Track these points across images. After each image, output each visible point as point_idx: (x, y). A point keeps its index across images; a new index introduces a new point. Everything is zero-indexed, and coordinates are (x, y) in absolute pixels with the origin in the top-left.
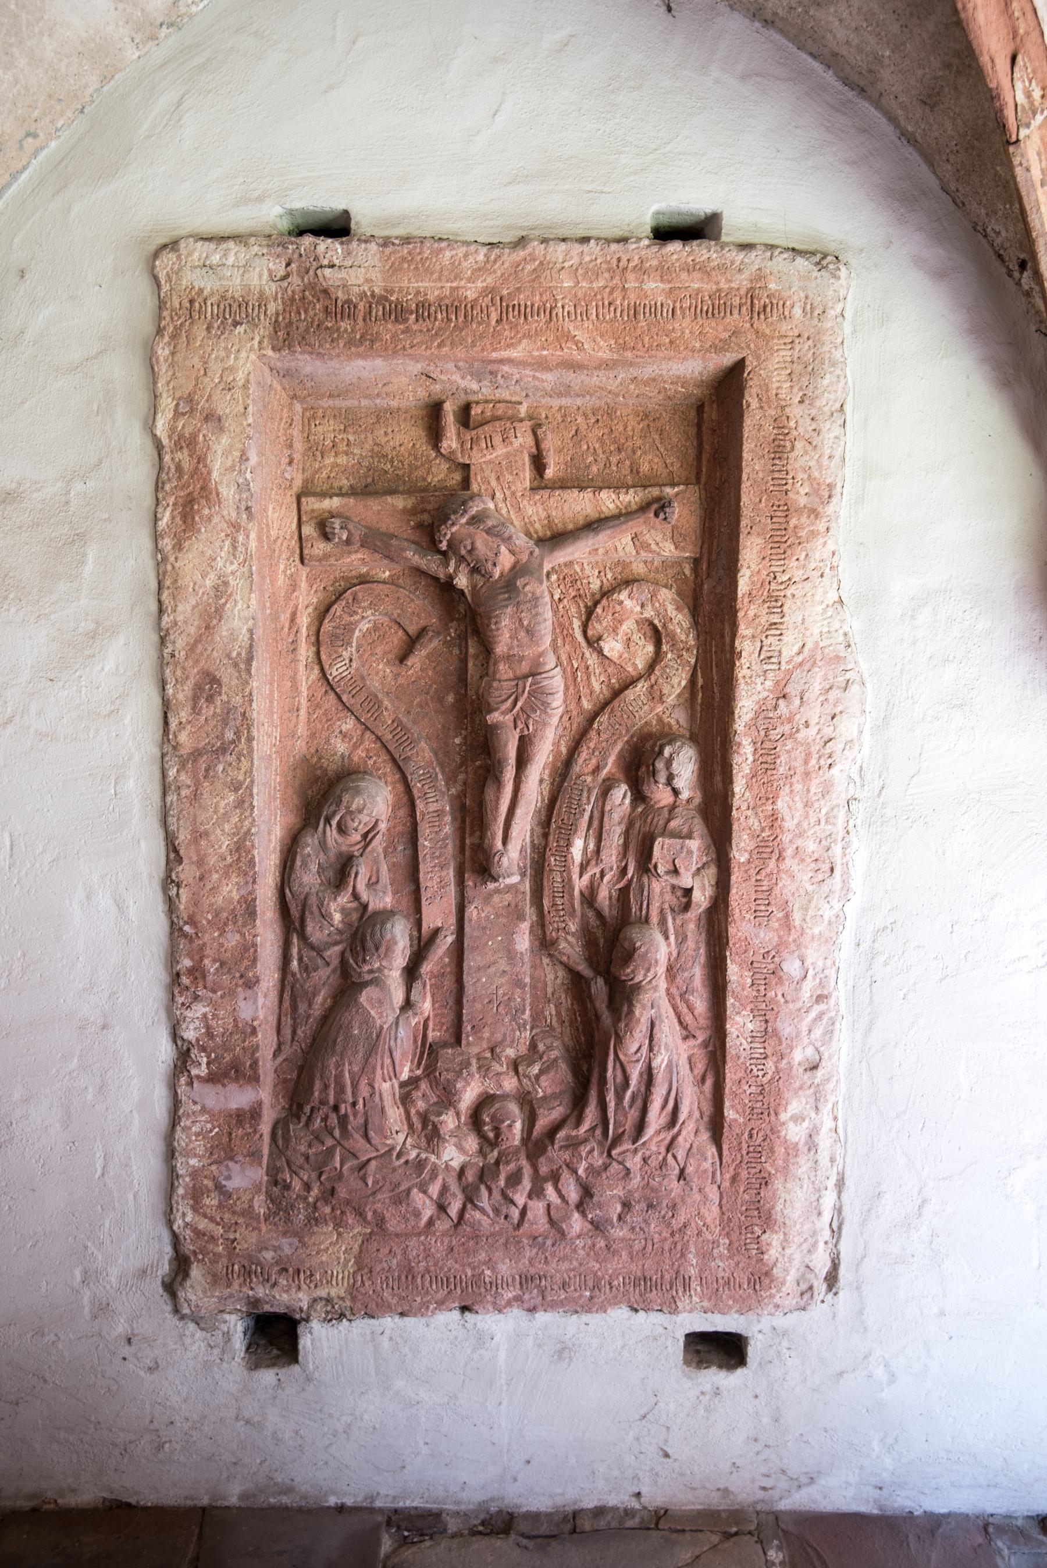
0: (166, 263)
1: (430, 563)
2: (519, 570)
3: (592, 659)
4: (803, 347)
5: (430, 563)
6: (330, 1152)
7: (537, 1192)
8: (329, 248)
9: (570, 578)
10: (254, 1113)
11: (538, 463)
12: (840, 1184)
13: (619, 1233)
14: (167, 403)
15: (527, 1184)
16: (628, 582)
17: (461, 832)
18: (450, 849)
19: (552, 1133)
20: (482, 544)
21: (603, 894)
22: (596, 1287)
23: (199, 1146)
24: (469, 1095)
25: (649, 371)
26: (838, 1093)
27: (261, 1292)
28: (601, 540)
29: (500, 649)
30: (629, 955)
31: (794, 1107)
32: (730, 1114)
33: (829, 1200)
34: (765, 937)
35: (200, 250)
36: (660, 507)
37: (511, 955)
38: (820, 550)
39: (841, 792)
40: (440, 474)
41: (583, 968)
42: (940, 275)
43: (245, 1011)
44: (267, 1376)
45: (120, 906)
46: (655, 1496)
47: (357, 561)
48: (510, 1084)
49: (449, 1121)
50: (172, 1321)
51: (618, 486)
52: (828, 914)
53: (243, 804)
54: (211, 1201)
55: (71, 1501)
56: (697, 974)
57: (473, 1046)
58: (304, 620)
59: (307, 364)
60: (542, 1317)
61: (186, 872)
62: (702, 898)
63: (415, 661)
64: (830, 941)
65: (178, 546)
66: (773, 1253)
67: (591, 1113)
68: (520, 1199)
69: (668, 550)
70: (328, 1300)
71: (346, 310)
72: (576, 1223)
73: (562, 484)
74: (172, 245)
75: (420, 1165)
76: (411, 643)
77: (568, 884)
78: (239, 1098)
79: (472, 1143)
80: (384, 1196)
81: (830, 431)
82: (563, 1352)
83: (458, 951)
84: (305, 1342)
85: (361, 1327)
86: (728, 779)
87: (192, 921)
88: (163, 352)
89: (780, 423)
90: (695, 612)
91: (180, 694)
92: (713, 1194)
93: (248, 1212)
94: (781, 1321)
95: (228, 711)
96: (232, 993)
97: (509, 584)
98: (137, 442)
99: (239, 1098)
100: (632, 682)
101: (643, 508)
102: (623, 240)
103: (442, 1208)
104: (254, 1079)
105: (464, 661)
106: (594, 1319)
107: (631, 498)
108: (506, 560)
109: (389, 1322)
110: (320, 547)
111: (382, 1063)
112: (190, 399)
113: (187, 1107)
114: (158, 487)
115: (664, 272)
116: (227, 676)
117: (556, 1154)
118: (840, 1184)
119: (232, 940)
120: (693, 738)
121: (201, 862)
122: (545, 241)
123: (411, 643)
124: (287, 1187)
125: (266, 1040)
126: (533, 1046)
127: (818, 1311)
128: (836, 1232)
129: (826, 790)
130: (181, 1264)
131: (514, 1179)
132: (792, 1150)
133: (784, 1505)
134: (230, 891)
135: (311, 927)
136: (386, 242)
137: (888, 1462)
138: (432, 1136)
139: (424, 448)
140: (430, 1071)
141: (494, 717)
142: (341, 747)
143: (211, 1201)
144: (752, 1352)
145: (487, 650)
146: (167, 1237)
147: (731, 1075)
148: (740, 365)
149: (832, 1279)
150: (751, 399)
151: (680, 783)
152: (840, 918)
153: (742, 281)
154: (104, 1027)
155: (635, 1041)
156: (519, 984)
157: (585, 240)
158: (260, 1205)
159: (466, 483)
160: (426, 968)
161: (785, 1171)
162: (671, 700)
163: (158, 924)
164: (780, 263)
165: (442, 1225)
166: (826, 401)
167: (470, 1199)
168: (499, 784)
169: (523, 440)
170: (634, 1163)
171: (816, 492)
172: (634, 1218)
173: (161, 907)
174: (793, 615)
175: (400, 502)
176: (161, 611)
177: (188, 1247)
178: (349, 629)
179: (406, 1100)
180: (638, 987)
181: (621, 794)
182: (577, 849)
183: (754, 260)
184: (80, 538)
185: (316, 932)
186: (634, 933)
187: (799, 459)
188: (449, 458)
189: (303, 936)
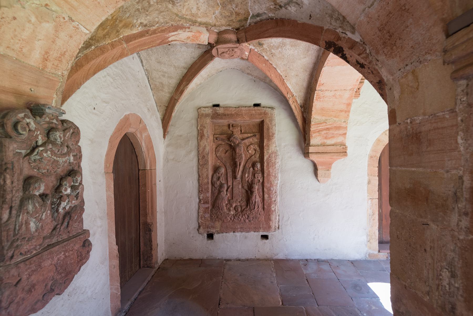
0: (199, 110)
1: (229, 142)
2: (239, 143)
3: (248, 153)
4: (270, 118)
5: (229, 142)
6: (217, 212)
7: (242, 217)
9: (245, 144)
10: (208, 208)
11: (241, 131)
12: (279, 216)
13: (252, 222)
14: (199, 125)
15: (241, 216)
16: (251, 144)
17: (233, 174)
18: (231, 176)
19: (244, 210)
20: (235, 140)
21: (250, 181)
22: (250, 229)
23: (202, 212)
24: (234, 205)
25: (253, 121)
26: (278, 204)
27: (209, 230)
28: (249, 139)
29: (237, 152)
30: (253, 187)
31: (273, 206)
32: (265, 207)
33: (277, 218)
34: (269, 185)
35: (203, 109)
36: (255, 136)
37: (239, 188)
38: (273, 140)
39: (277, 168)
40: (230, 132)
41: (247, 190)
42: (286, 110)
43: (207, 195)
44: (210, 241)
45: (193, 183)
46: (258, 257)
47: (220, 142)
48: (239, 204)
49: (232, 209)
50: (198, 234)
51: (250, 133)
52: (276, 182)
53: (208, 170)
54: (203, 219)
55: (185, 258)
56: (261, 190)
57: (234, 200)
58: (214, 149)
59: (215, 121)
60: (243, 233)
61: (201, 179)
62: (261, 181)
63: (227, 154)
64: (276, 186)
65: (200, 141)
66: (271, 224)
67: (249, 207)
68: (240, 218)
69: (256, 140)
70: (217, 231)
71: (219, 115)
72: (247, 221)
73: (244, 133)
74: (200, 108)
75: (228, 214)
76: (226, 152)
77: (245, 180)
78: (207, 206)
79: (234, 211)
80: (224, 217)
81: (274, 127)
82: (246, 238)
83: (232, 188)
84: (214, 237)
85: (221, 234)
86: (264, 167)
87: (201, 184)
88: (199, 120)
89: (268, 126)
90: (260, 147)
91: (200, 158)
92: (263, 217)
93: (208, 220)
94: (272, 233)
95: (206, 160)
96: (206, 193)
97: (238, 145)
98: (195, 129)
99: (207, 206)
100: (253, 156)
101: (253, 136)
102: (250, 107)
103: (231, 219)
104: (208, 203)
105: (233, 153)
106: (250, 233)
107: (252, 135)
108: (237, 142)
109: (224, 234)
110: (216, 141)
111: (224, 201)
112: (202, 125)
113: (201, 207)
114: (198, 135)
115: (255, 110)
116: (206, 156)
117: (244, 212)
118: (279, 216)
119: (206, 186)
120: (260, 162)
121: (202, 177)
122: (241, 107)
123: (226, 152)
124: (212, 217)
125: (210, 199)
126: (242, 199)
127: (277, 232)
128: (279, 222)
129: (275, 168)
130: (199, 227)
131: (240, 215)
132: (273, 211)
133: (274, 258)
134: (206, 181)
135: (215, 185)
136: (224, 107)
137: (287, 252)
138: (229, 210)
139: (228, 129)
140: (229, 203)
141: (236, 160)
142: (218, 164)
143: (203, 219)
144: (269, 237)
145: (235, 152)
146: (198, 223)
147: (265, 202)
148: (263, 120)
149: (278, 228)
150: (265, 124)
151: (258, 167)
152: (277, 183)
153: (263, 111)
154: (191, 197)
155: (254, 198)
156: (240, 192)
157: (246, 107)
158: (209, 219)
159: (233, 133)
160: (229, 190)
161: (272, 214)
162: (257, 158)
163: (197, 185)
164: (267, 109)
165: (231, 221)
166: (273, 124)
167: (234, 218)
168: (237, 168)
169: (239, 128)
170: (254, 213)
171: (272, 134)
172: (254, 220)
173: (197, 183)
174: (270, 148)
175: (225, 135)
176: (198, 148)
177: (200, 224)
178: (219, 150)
179: (226, 206)
180: (254, 191)
181: (251, 169)
182: (246, 175)
183: (265, 109)
184: (189, 140)
185: (216, 186)
186: (253, 185)
187: (270, 130)
188: (231, 130)
189: (214, 186)
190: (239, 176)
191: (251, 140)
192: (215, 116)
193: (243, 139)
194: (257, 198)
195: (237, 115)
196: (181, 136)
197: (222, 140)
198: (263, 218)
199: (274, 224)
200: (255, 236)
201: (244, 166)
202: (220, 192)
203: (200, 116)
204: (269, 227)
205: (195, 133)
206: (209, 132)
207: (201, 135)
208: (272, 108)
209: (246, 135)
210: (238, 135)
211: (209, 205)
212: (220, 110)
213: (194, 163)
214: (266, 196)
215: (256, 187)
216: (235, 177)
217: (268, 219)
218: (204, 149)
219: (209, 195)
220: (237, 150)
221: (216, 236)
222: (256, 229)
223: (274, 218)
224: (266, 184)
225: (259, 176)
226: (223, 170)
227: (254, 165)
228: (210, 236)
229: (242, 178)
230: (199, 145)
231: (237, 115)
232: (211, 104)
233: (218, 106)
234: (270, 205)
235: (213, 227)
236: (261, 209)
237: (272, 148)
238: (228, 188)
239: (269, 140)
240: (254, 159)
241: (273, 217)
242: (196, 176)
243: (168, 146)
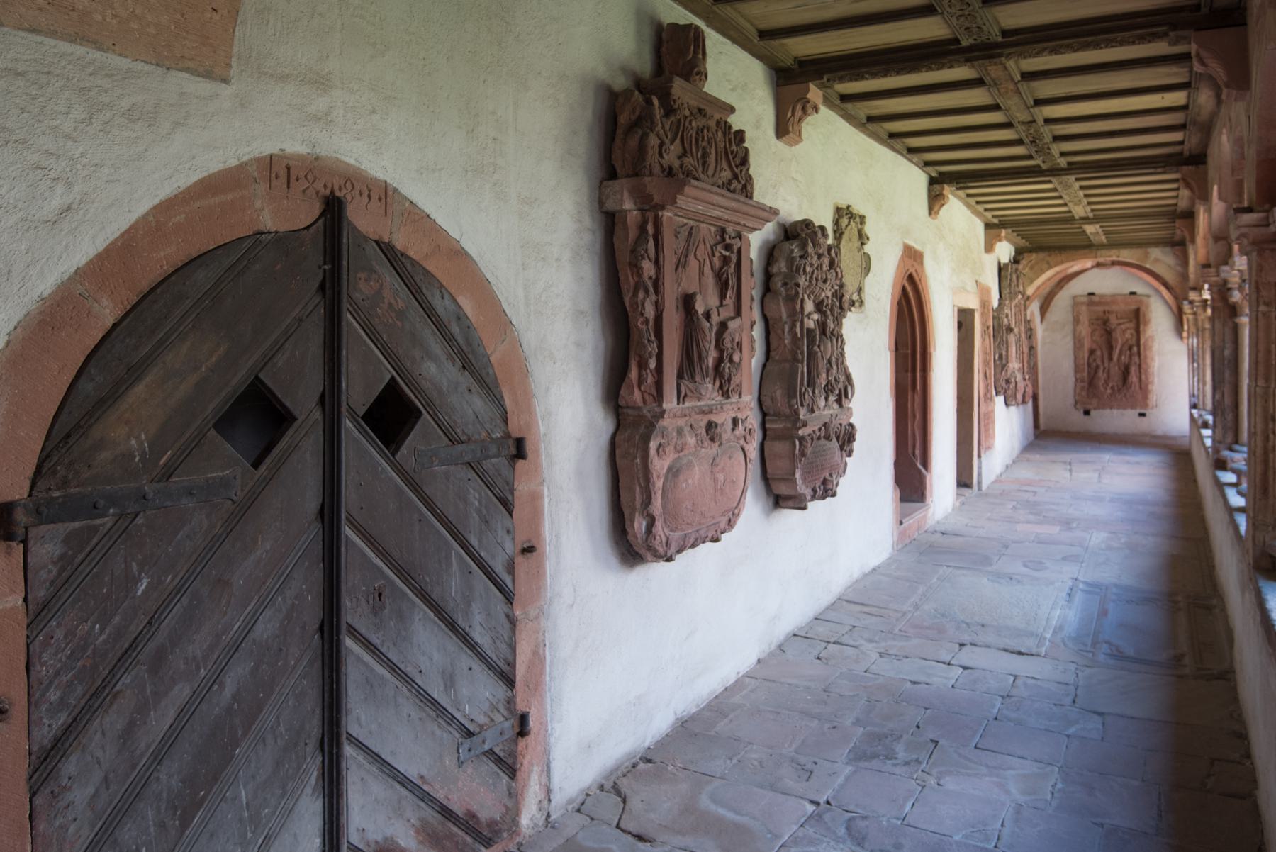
8: (1093, 297)
24: (1110, 385)
36: (1131, 321)
40: (1105, 318)
64: (1154, 367)
99: (1082, 384)
130: (1076, 403)
138: (1106, 389)
155: (1130, 378)
169: (1115, 315)
181: (1128, 352)
190: (1115, 357)
191: (1127, 325)
192: (1091, 304)
193: (1119, 324)
194: (1133, 378)
201: (1121, 350)
202: (1096, 372)
203: (1076, 303)
205: (1071, 318)
206: (1084, 319)
207: (1076, 321)
208: (1148, 296)
209: (1122, 321)
210: (1113, 321)
211: (1086, 384)
212: (1095, 299)
213: (1071, 345)
214: (1143, 377)
215: (1133, 369)
216: (1111, 359)
218: (1080, 332)
219: (1085, 374)
220: (1114, 335)
221: (1093, 413)
222: (1133, 407)
223: (1153, 398)
224: (1143, 366)
225: (1136, 359)
226: (1099, 353)
227: (1130, 348)
228: (1087, 413)
230: (1074, 330)
232: (1086, 293)
234: (1147, 386)
236: (1137, 388)
238: (1104, 369)
241: (1150, 396)
242: (1072, 357)
243: (1046, 330)
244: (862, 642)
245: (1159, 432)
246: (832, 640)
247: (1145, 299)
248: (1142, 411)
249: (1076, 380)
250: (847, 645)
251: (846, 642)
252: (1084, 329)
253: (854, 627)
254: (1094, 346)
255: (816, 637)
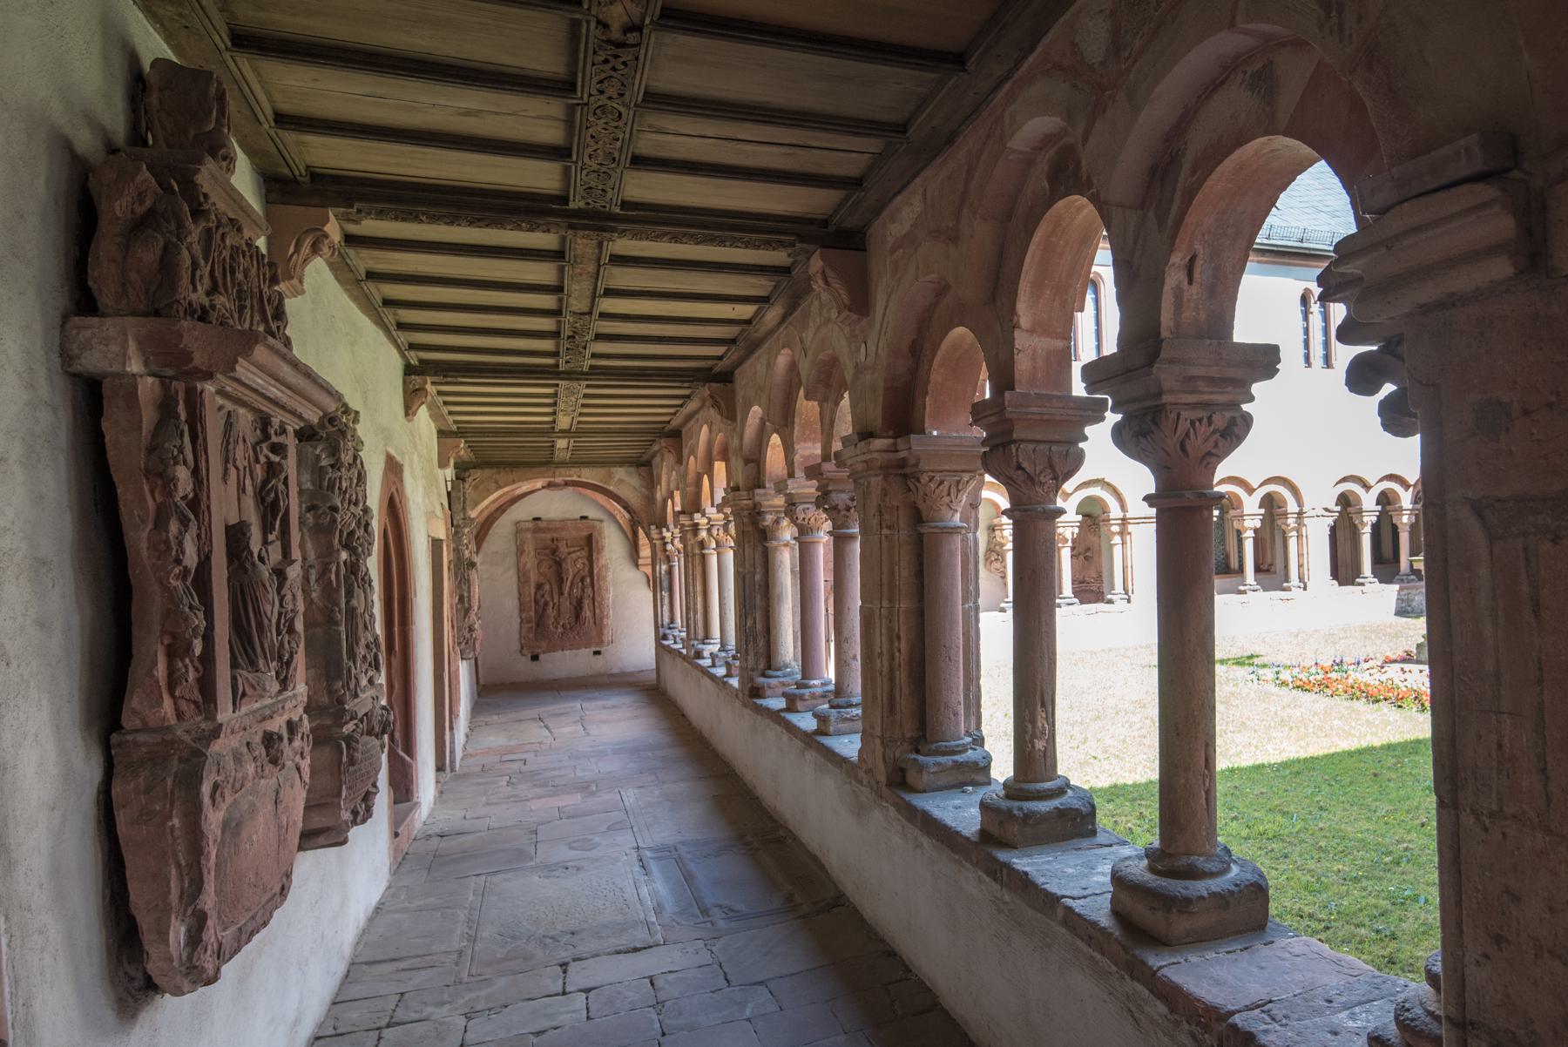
2: (566, 558)
8: (539, 522)
47: (543, 557)
74: (518, 522)
76: (550, 567)
78: (530, 625)
82: (576, 655)
99: (530, 625)
123: (550, 567)
130: (522, 648)
138: (556, 628)
190: (566, 590)
191: (578, 554)
192: (537, 530)
193: (569, 553)
194: (587, 613)
195: (562, 529)
196: (497, 552)
197: (546, 555)
198: (594, 633)
199: (607, 638)
200: (584, 654)
201: (572, 582)
202: (544, 609)
203: (519, 529)
204: (602, 642)
205: (514, 549)
206: (529, 548)
207: (520, 551)
208: (601, 521)
209: (573, 549)
210: (563, 549)
211: (534, 625)
212: (542, 525)
213: (514, 579)
214: (597, 610)
215: (586, 602)
216: (561, 593)
217: (600, 633)
218: (526, 564)
219: (532, 613)
220: (564, 565)
221: (542, 657)
224: (597, 598)
225: (589, 591)
226: (547, 587)
227: (582, 580)
229: (570, 594)
231: (562, 529)
232: (531, 518)
233: (539, 519)
234: (601, 620)
235: (539, 647)
237: (603, 561)
238: (554, 605)
239: (598, 553)
240: (582, 573)
241: (606, 632)
244: (430, 1009)
245: (616, 670)
246: (383, 1023)
247: (597, 523)
248: (597, 649)
249: (522, 620)
250: (412, 1022)
251: (406, 1018)
252: (530, 560)
253: (402, 994)
254: (542, 580)
255: (354, 1029)
